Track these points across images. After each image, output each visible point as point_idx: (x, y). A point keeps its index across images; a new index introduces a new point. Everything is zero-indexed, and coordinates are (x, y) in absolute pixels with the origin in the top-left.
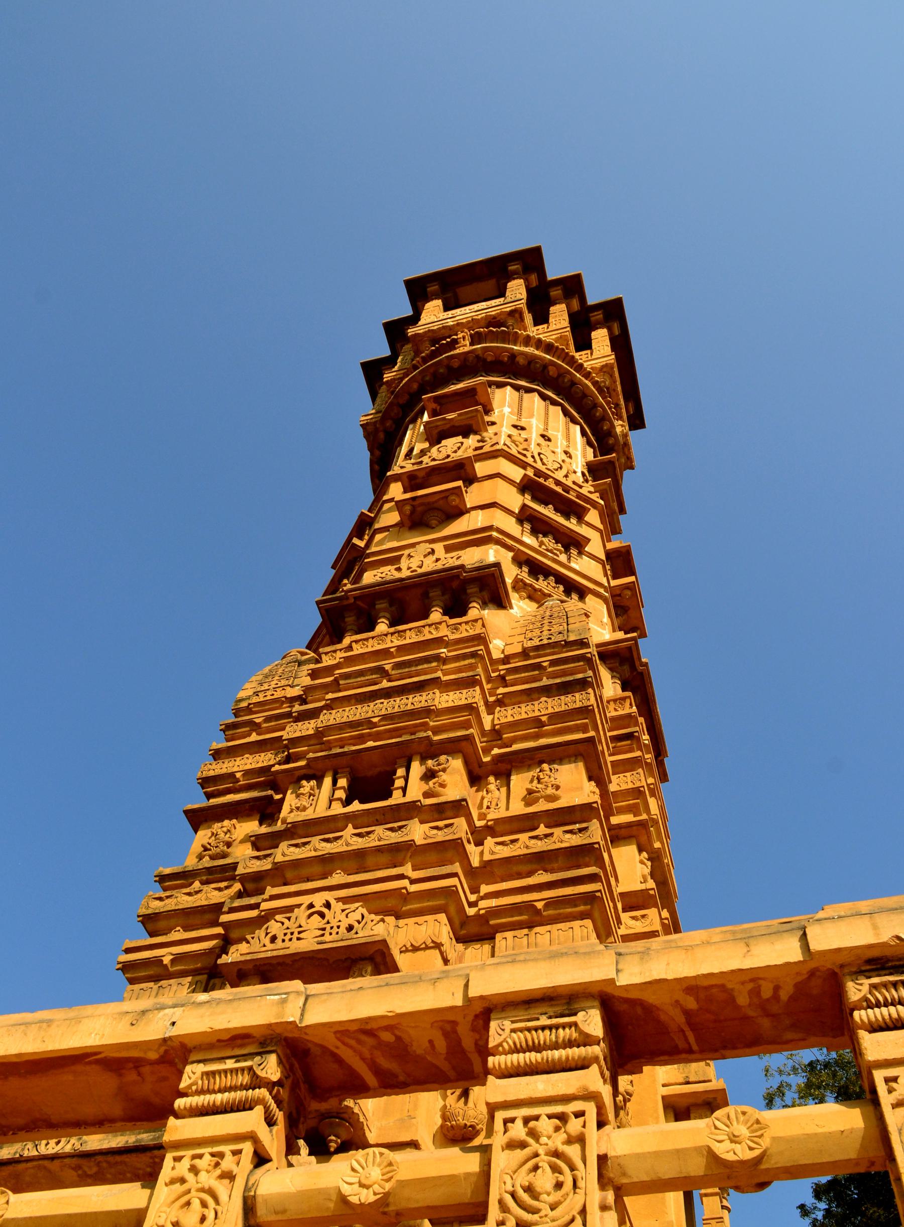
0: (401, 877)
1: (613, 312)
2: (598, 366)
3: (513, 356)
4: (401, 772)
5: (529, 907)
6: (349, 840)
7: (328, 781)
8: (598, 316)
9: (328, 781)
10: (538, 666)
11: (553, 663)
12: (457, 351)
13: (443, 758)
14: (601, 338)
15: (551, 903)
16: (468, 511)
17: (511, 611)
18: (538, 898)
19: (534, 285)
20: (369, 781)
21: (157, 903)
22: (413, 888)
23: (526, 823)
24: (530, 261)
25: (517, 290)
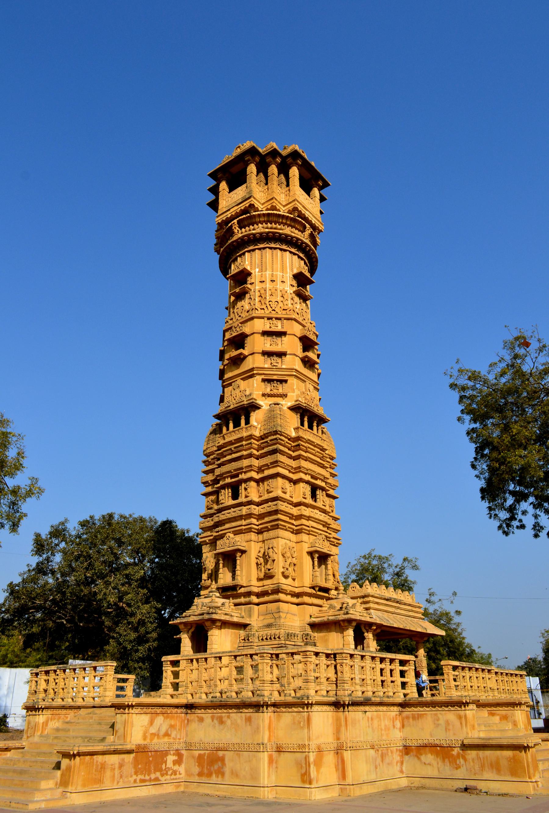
0: (242, 525)
1: (295, 155)
2: (291, 209)
3: (254, 235)
5: (267, 527)
6: (232, 513)
7: (226, 490)
8: (289, 160)
9: (226, 490)
10: (267, 442)
11: (271, 440)
12: (235, 238)
13: (248, 483)
14: (294, 172)
15: (271, 526)
16: (247, 356)
17: (263, 408)
18: (268, 525)
19: (258, 160)
21: (202, 525)
22: (244, 527)
23: (266, 501)
24: (252, 151)
25: (252, 168)
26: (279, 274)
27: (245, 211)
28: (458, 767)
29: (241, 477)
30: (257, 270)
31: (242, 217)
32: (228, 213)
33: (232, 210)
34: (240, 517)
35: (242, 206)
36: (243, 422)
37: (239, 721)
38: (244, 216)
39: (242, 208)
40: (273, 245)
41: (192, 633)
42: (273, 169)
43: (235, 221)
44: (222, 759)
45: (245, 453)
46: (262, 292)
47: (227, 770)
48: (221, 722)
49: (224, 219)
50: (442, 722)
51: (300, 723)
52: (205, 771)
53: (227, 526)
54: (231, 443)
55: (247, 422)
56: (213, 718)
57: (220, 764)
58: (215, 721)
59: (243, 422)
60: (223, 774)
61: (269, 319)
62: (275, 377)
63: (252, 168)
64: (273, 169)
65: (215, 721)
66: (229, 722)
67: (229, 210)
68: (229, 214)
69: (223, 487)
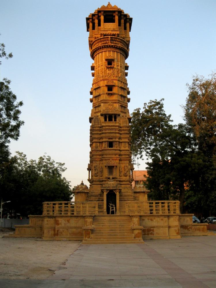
2: (128, 40)
3: (117, 46)
4: (113, 143)
7: (107, 142)
20: (111, 145)
25: (117, 18)
26: (122, 64)
27: (114, 35)
28: (189, 231)
29: (113, 140)
30: (116, 60)
31: (113, 37)
32: (107, 32)
33: (109, 32)
34: (116, 155)
35: (114, 33)
36: (113, 119)
37: (158, 220)
38: (113, 37)
39: (114, 33)
40: (121, 52)
41: (108, 193)
42: (122, 21)
43: (109, 37)
44: (153, 230)
45: (117, 131)
46: (118, 70)
47: (155, 233)
48: (152, 220)
49: (105, 33)
50: (186, 220)
51: (176, 220)
52: (146, 233)
53: (108, 156)
54: (109, 126)
55: (115, 120)
56: (148, 219)
57: (152, 231)
58: (149, 220)
59: (113, 119)
60: (153, 234)
61: (121, 82)
62: (124, 105)
63: (117, 18)
64: (122, 21)
65: (149, 220)
66: (155, 220)
67: (107, 31)
68: (107, 33)
69: (105, 142)
